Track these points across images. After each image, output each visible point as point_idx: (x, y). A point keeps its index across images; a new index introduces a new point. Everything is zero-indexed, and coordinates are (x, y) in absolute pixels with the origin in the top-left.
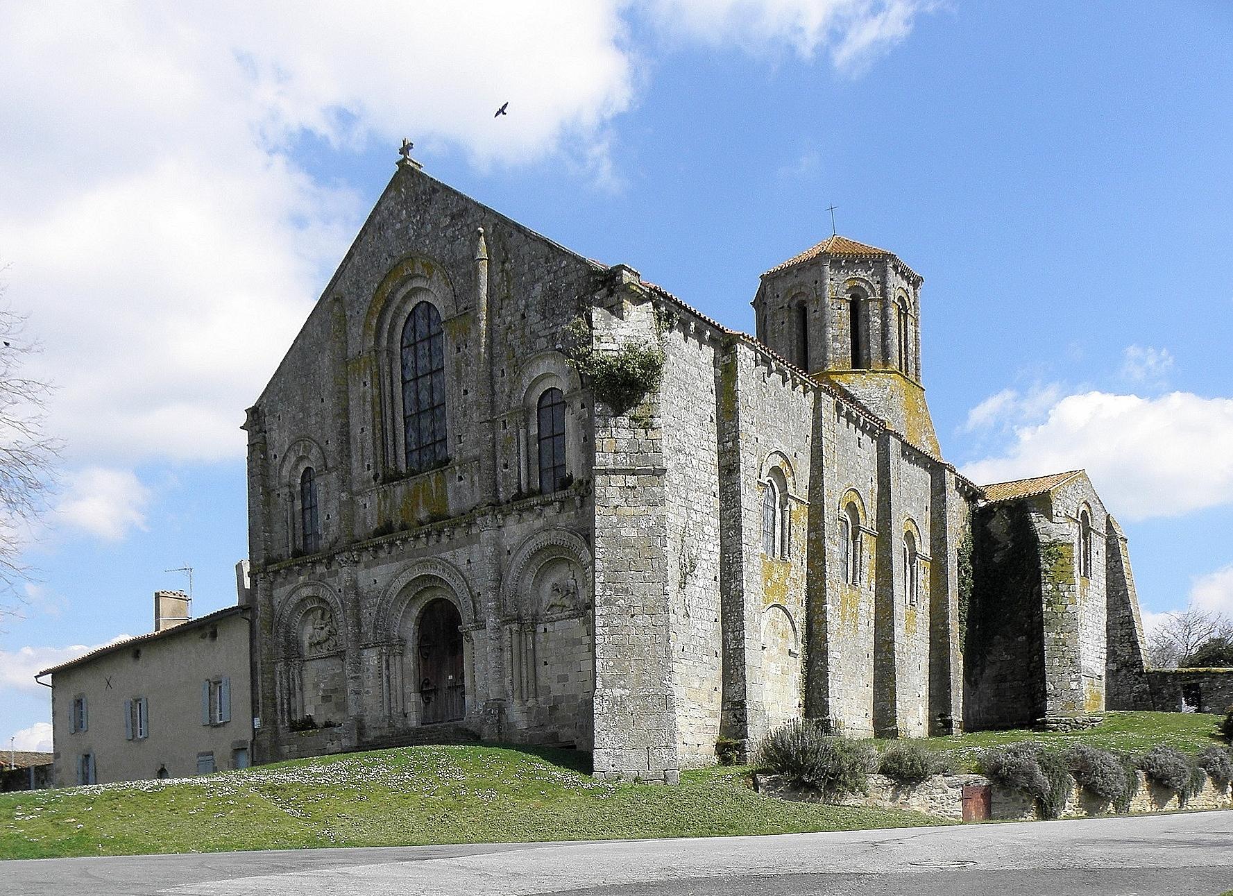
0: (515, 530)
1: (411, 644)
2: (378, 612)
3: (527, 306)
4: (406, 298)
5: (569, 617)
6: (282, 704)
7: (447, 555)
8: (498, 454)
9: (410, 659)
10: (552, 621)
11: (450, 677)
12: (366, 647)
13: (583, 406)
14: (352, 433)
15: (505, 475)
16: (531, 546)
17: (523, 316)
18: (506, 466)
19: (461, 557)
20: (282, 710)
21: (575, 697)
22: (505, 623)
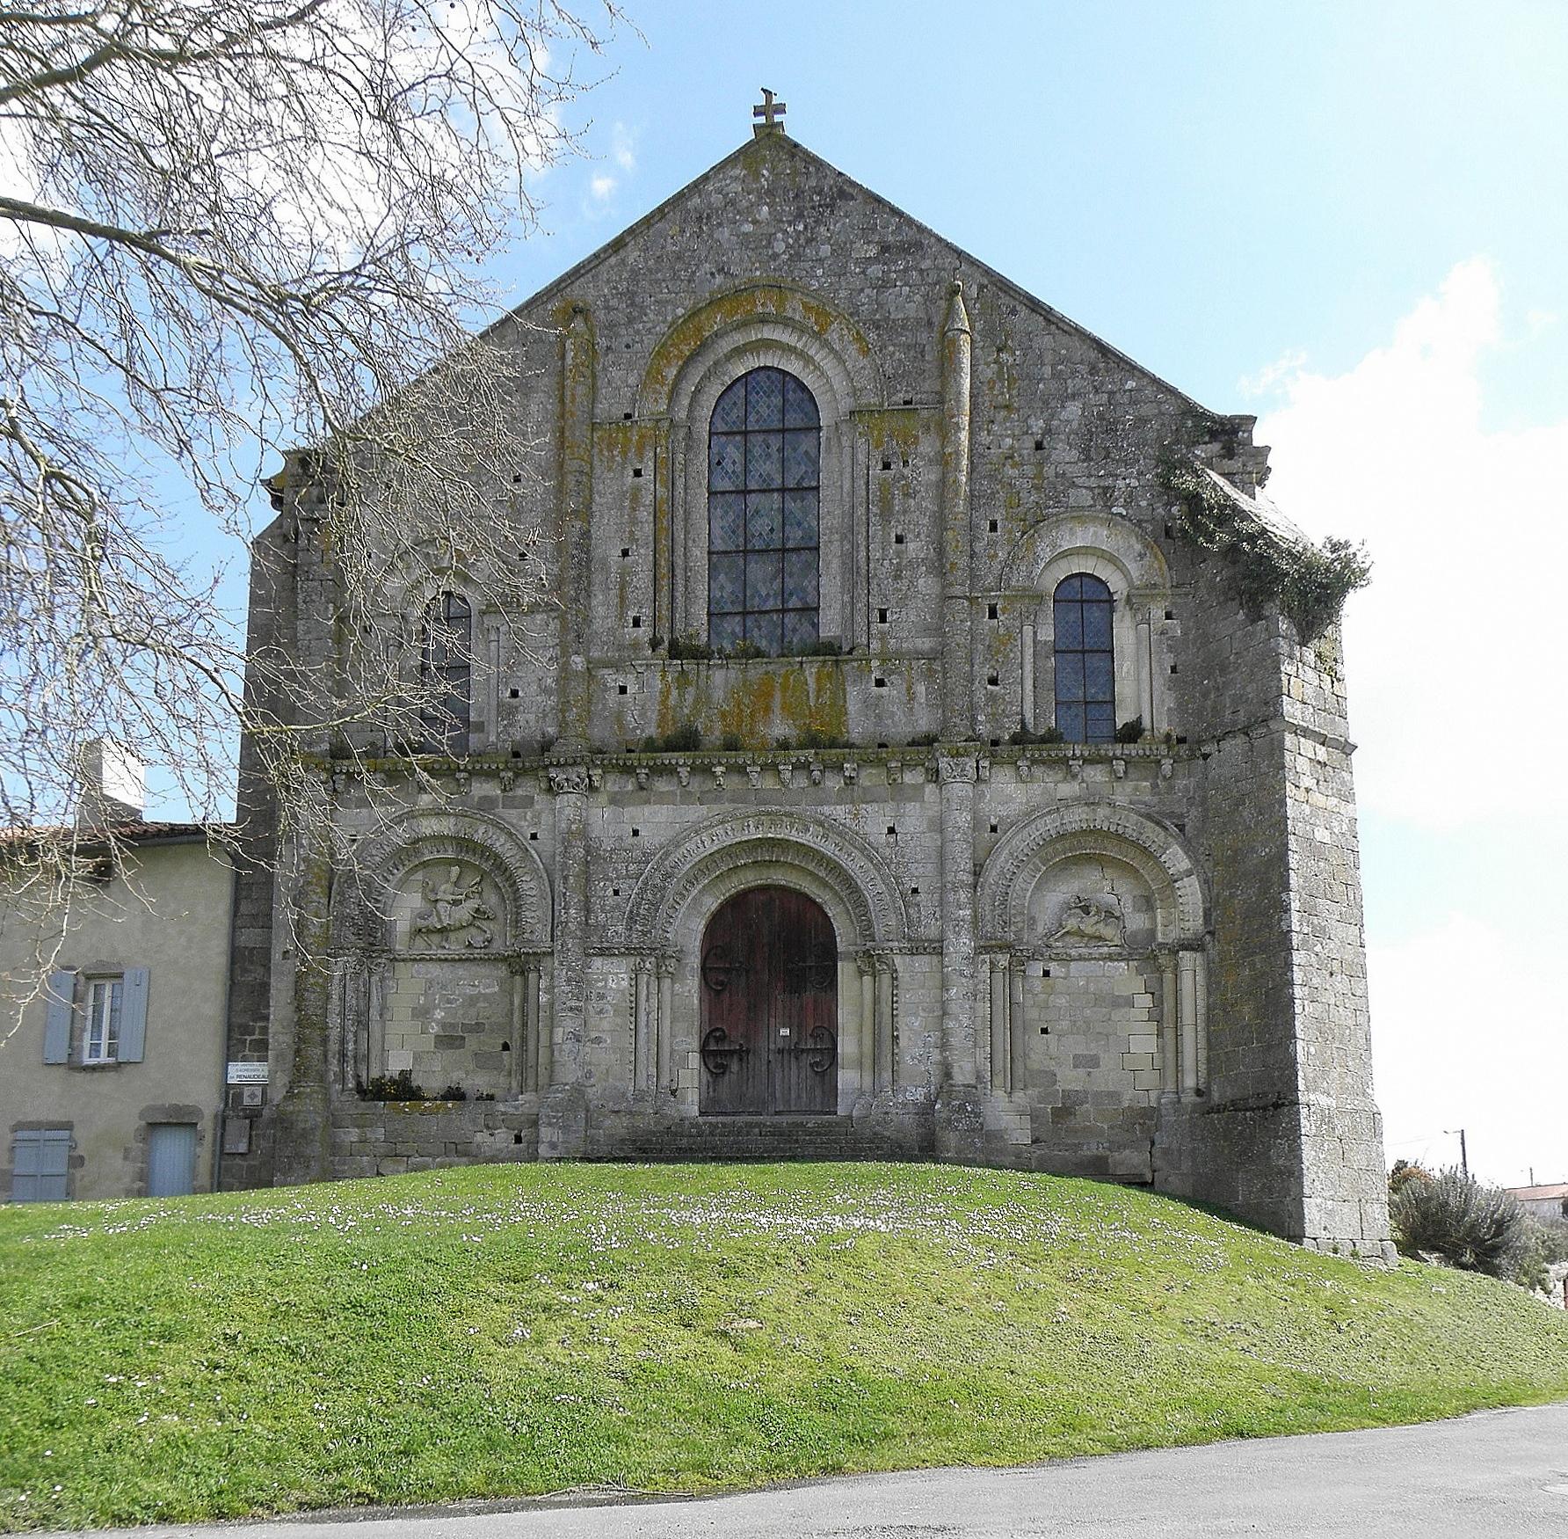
0: (1009, 793)
1: (694, 961)
2: (643, 890)
3: (1048, 431)
4: (739, 352)
5: (1110, 958)
6: (343, 1041)
7: (840, 812)
8: (978, 660)
9: (689, 988)
10: (1065, 960)
11: (785, 1032)
12: (603, 953)
13: (1169, 616)
14: (597, 553)
15: (992, 698)
16: (1049, 825)
17: (1039, 446)
18: (993, 681)
19: (875, 821)
20: (343, 1055)
21: (1114, 1096)
22: (987, 949)
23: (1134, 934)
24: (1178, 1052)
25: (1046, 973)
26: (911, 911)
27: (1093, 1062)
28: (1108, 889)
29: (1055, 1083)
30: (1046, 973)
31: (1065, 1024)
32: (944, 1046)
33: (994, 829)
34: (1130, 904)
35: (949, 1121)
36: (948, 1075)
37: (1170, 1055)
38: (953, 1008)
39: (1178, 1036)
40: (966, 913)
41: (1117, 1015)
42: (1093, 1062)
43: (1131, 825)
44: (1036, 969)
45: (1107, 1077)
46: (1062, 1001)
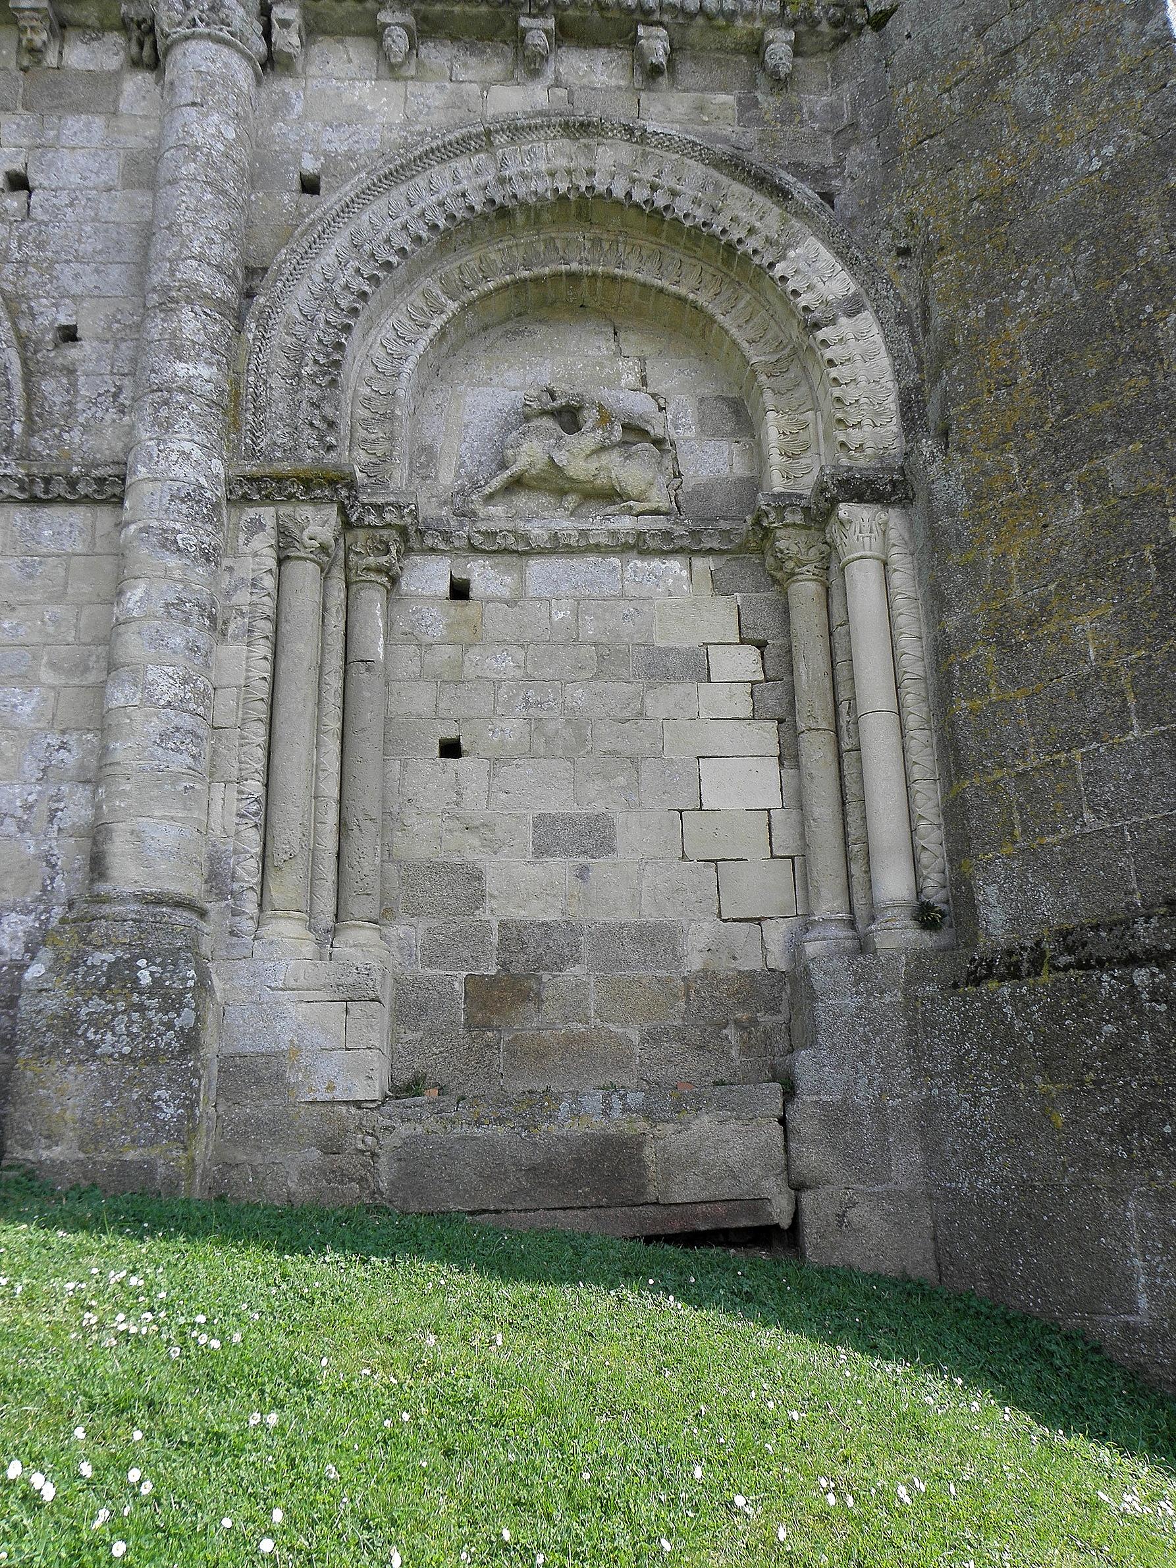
5: (638, 546)
21: (658, 939)
23: (703, 493)
24: (849, 799)
25: (460, 591)
26: (47, 386)
27: (594, 837)
28: (631, 379)
29: (477, 900)
30: (460, 591)
31: (511, 729)
32: (97, 775)
33: (310, 186)
34: (690, 416)
35: (68, 1024)
36: (97, 865)
37: (823, 809)
38: (133, 646)
39: (846, 753)
40: (200, 373)
41: (660, 703)
42: (594, 837)
43: (689, 188)
44: (429, 576)
45: (636, 883)
46: (503, 664)
